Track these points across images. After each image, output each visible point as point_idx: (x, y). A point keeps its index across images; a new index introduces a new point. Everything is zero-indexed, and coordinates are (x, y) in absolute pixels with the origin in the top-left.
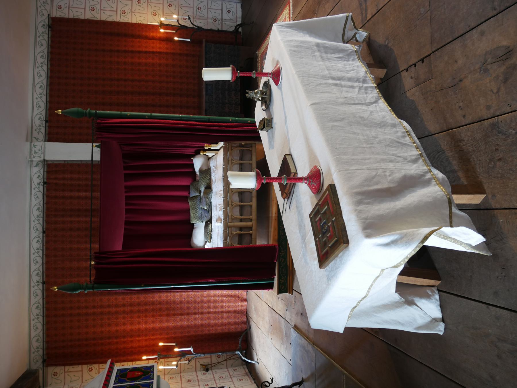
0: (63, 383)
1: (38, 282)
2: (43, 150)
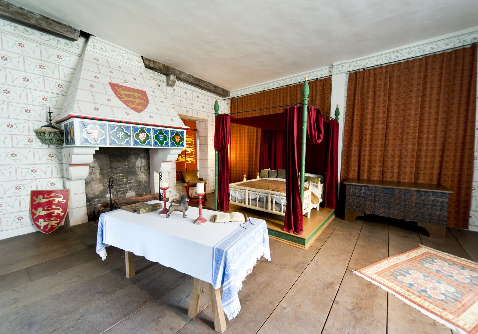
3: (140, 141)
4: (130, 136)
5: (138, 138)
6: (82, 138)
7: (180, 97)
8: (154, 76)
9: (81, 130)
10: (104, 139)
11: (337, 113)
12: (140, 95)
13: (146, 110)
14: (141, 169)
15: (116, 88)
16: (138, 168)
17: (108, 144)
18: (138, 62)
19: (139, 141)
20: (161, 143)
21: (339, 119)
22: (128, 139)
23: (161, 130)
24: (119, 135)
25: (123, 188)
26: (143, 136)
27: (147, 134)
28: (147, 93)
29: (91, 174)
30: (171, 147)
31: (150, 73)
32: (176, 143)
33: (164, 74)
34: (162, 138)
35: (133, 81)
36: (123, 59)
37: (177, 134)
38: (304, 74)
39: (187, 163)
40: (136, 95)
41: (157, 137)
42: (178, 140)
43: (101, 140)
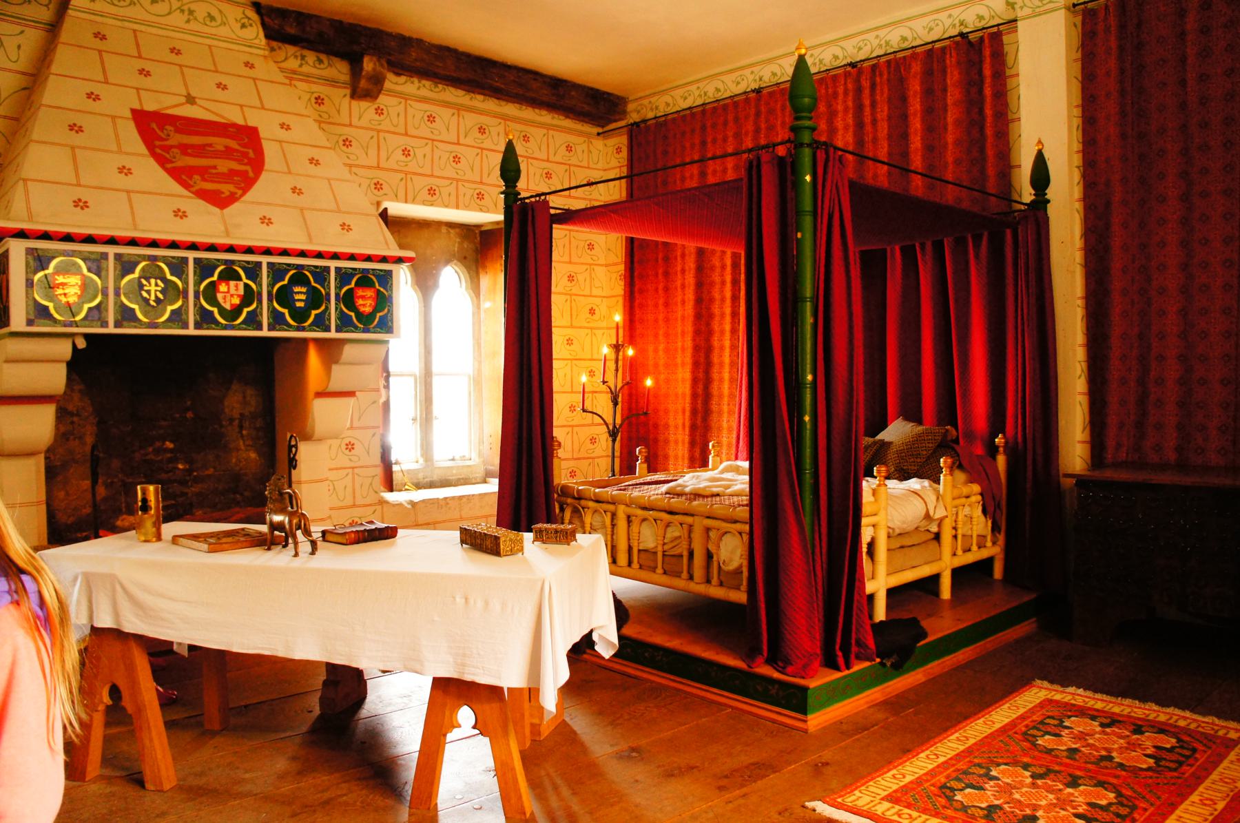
0: (607, 166)
1: (761, 79)
2: (1042, 9)
3: (222, 311)
4: (185, 294)
5: (213, 301)
6: (31, 303)
7: (406, 134)
8: (301, 66)
9: (31, 276)
10: (98, 307)
11: (1041, 177)
12: (233, 144)
13: (250, 196)
14: (241, 427)
15: (154, 126)
16: (231, 420)
17: (111, 320)
18: (243, 26)
19: (215, 310)
20: (300, 316)
21: (1048, 201)
22: (179, 303)
23: (300, 267)
24: (148, 292)
26: (230, 293)
27: (246, 286)
28: (262, 134)
29: (68, 439)
30: (337, 331)
31: (286, 59)
32: (360, 316)
33: (341, 55)
34: (303, 297)
35: (220, 94)
36: (188, 21)
37: (365, 280)
38: (909, 19)
40: (219, 143)
41: (284, 296)
42: (366, 305)
43: (90, 309)
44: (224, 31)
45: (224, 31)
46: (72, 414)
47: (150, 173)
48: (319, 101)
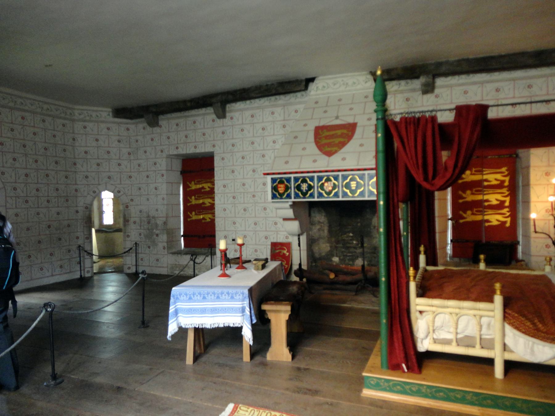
3: (326, 193)
5: (323, 189)
12: (345, 131)
18: (366, 82)
25: (352, 253)
34: (355, 185)
39: (487, 224)
40: (339, 132)
44: (359, 87)
45: (359, 87)
46: (321, 223)
47: (313, 148)
48: (407, 100)
